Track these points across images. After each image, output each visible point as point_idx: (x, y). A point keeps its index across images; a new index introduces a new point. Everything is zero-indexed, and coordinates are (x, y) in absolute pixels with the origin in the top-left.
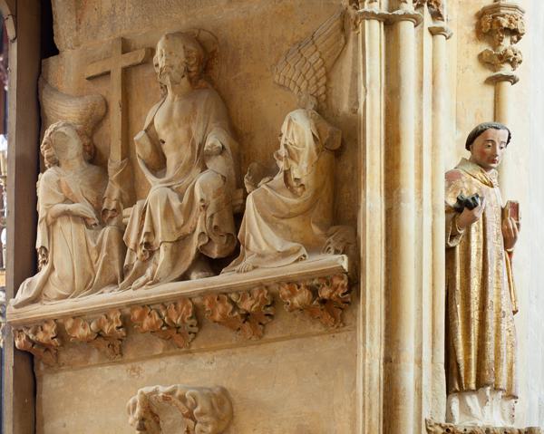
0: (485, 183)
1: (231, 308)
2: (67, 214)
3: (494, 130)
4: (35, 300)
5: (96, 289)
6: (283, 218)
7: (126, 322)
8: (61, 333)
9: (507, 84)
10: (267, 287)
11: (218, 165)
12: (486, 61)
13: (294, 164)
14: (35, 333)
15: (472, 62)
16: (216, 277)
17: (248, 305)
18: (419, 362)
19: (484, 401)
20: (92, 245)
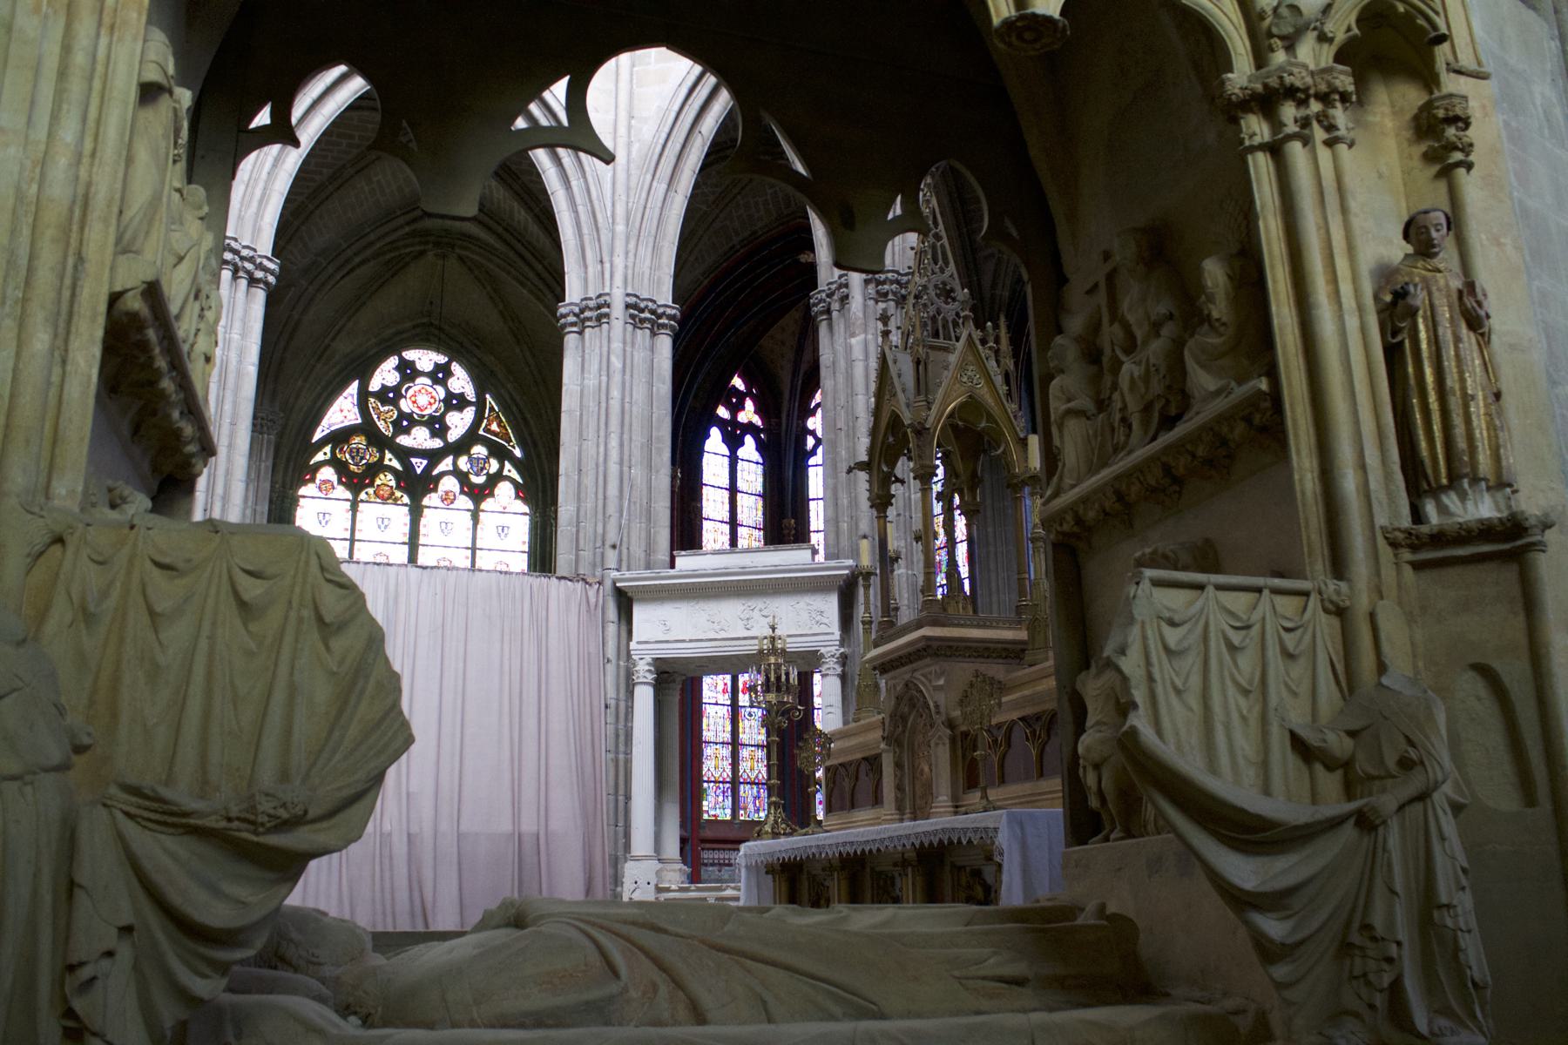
0: (1430, 270)
1: (1189, 458)
2: (1069, 412)
3: (1422, 216)
4: (1056, 495)
5: (1097, 471)
6: (1216, 360)
7: (1120, 497)
8: (1079, 521)
9: (1462, 171)
10: (1211, 429)
11: (1168, 330)
12: (1429, 157)
13: (1211, 306)
14: (1061, 525)
15: (1417, 163)
16: (1172, 433)
17: (1201, 451)
18: (1362, 466)
19: (1463, 497)
20: (1091, 432)
